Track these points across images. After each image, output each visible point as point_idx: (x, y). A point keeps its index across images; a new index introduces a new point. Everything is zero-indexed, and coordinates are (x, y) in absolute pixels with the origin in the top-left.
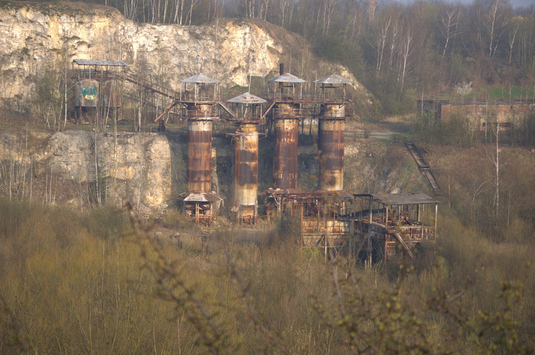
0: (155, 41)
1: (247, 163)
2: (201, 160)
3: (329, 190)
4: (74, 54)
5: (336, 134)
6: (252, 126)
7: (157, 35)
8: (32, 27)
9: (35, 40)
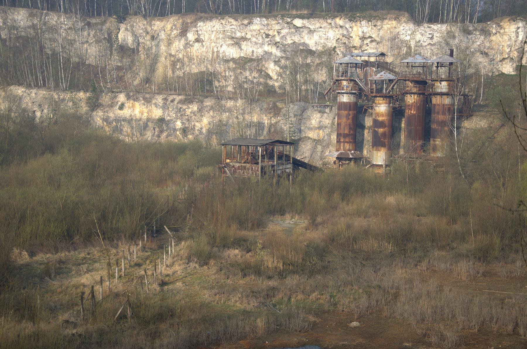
0: (429, 38)
1: (376, 129)
2: (341, 125)
3: (432, 155)
4: (366, 50)
5: (437, 107)
6: (382, 99)
7: (431, 33)
8: (341, 31)
9: (341, 40)
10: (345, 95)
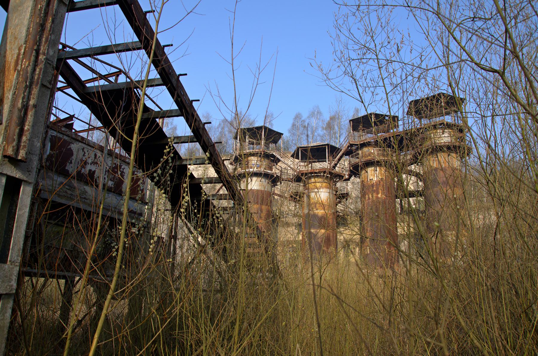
10: (254, 179)
